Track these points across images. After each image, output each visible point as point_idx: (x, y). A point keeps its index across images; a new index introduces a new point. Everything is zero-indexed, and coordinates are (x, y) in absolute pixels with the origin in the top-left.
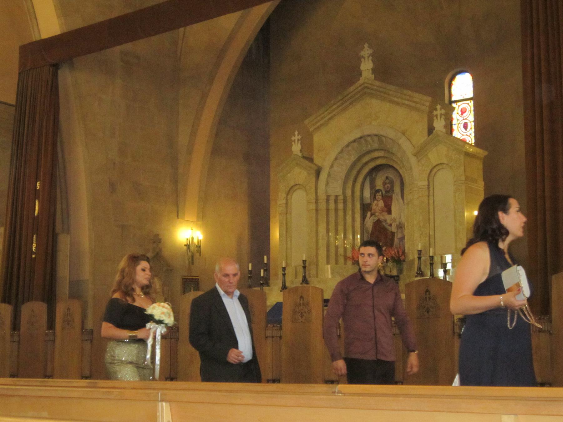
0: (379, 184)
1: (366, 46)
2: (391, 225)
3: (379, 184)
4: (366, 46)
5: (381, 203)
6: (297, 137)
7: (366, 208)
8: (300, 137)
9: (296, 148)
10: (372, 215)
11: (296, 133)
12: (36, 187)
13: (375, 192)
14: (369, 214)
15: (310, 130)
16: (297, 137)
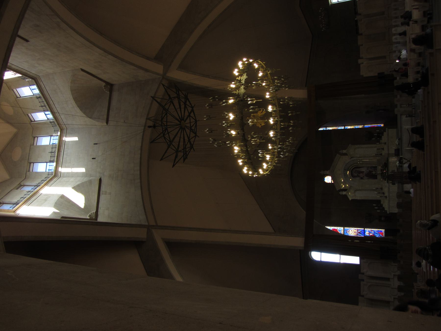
0: (356, 175)
1: (320, 172)
2: (367, 172)
3: (356, 175)
4: (320, 172)
5: (361, 174)
6: (341, 193)
7: (362, 178)
8: (341, 192)
9: (344, 193)
10: (364, 177)
11: (340, 193)
12: (350, 241)
13: (358, 176)
14: (364, 178)
15: (339, 189)
16: (341, 193)
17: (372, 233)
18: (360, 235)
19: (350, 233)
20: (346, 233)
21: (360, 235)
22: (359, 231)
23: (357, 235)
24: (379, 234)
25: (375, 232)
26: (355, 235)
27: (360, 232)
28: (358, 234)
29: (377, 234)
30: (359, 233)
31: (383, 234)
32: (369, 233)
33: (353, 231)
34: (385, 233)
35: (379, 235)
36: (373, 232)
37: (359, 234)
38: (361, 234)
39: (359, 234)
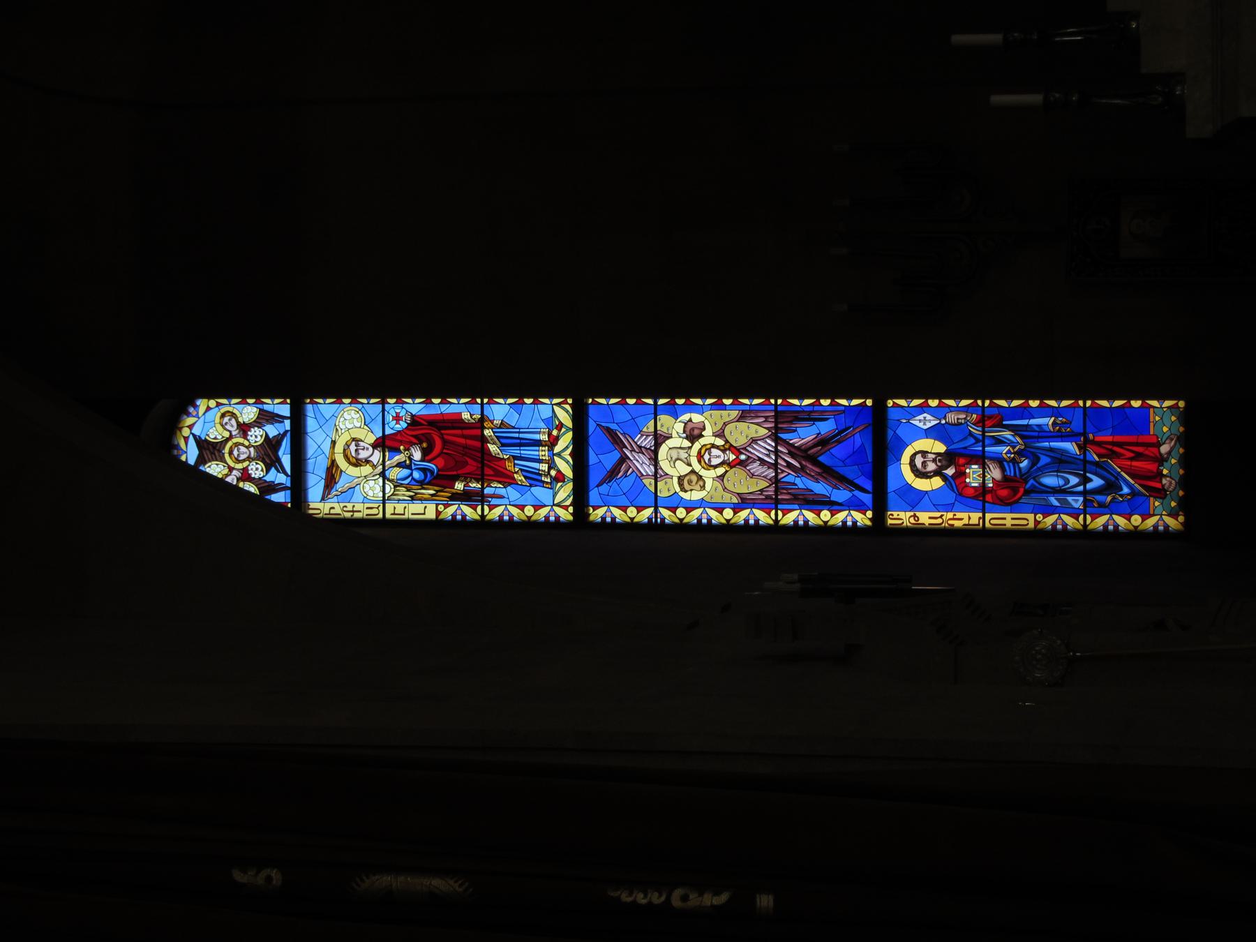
17: (1000, 461)
18: (820, 488)
19: (664, 465)
20: (612, 474)
21: (820, 488)
22: (804, 435)
23: (776, 498)
24: (1099, 468)
25: (1042, 434)
26: (744, 502)
27: (823, 442)
28: (790, 477)
29: (1061, 462)
30: (801, 471)
31: (1161, 460)
32: (949, 458)
33: (708, 438)
34: (1184, 440)
35: (1096, 482)
36: (1006, 444)
37: (801, 483)
38: (828, 473)
39: (801, 483)
